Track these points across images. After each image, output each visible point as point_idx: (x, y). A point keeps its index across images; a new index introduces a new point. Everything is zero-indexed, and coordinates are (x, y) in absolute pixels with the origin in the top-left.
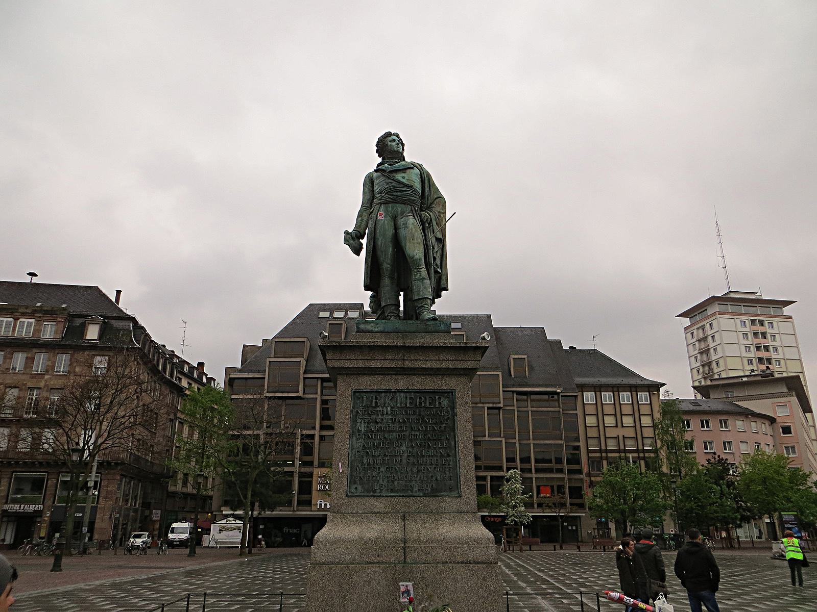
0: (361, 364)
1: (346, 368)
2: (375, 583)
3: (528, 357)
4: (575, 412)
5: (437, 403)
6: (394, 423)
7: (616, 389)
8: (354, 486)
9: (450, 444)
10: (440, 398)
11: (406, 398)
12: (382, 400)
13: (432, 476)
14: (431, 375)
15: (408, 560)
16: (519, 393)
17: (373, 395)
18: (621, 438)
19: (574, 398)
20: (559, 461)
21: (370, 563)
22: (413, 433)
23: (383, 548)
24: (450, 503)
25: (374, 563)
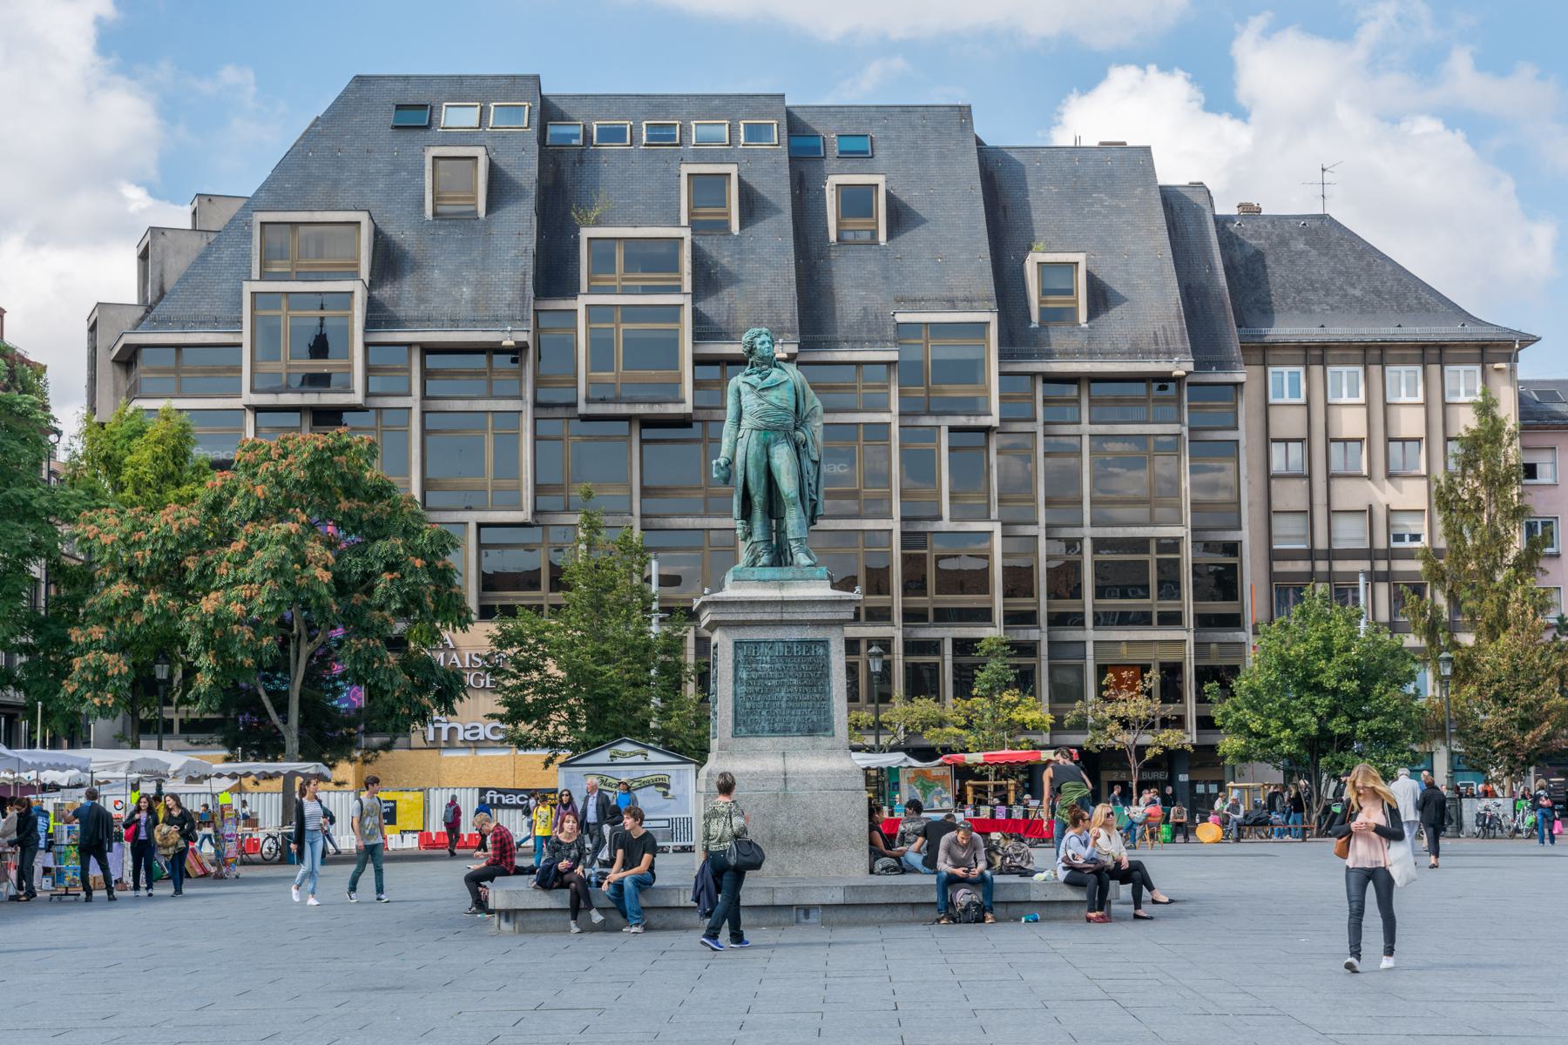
0: (741, 617)
4: (1230, 435)
7: (1374, 354)
15: (789, 788)
16: (1050, 379)
19: (1231, 387)
24: (824, 741)
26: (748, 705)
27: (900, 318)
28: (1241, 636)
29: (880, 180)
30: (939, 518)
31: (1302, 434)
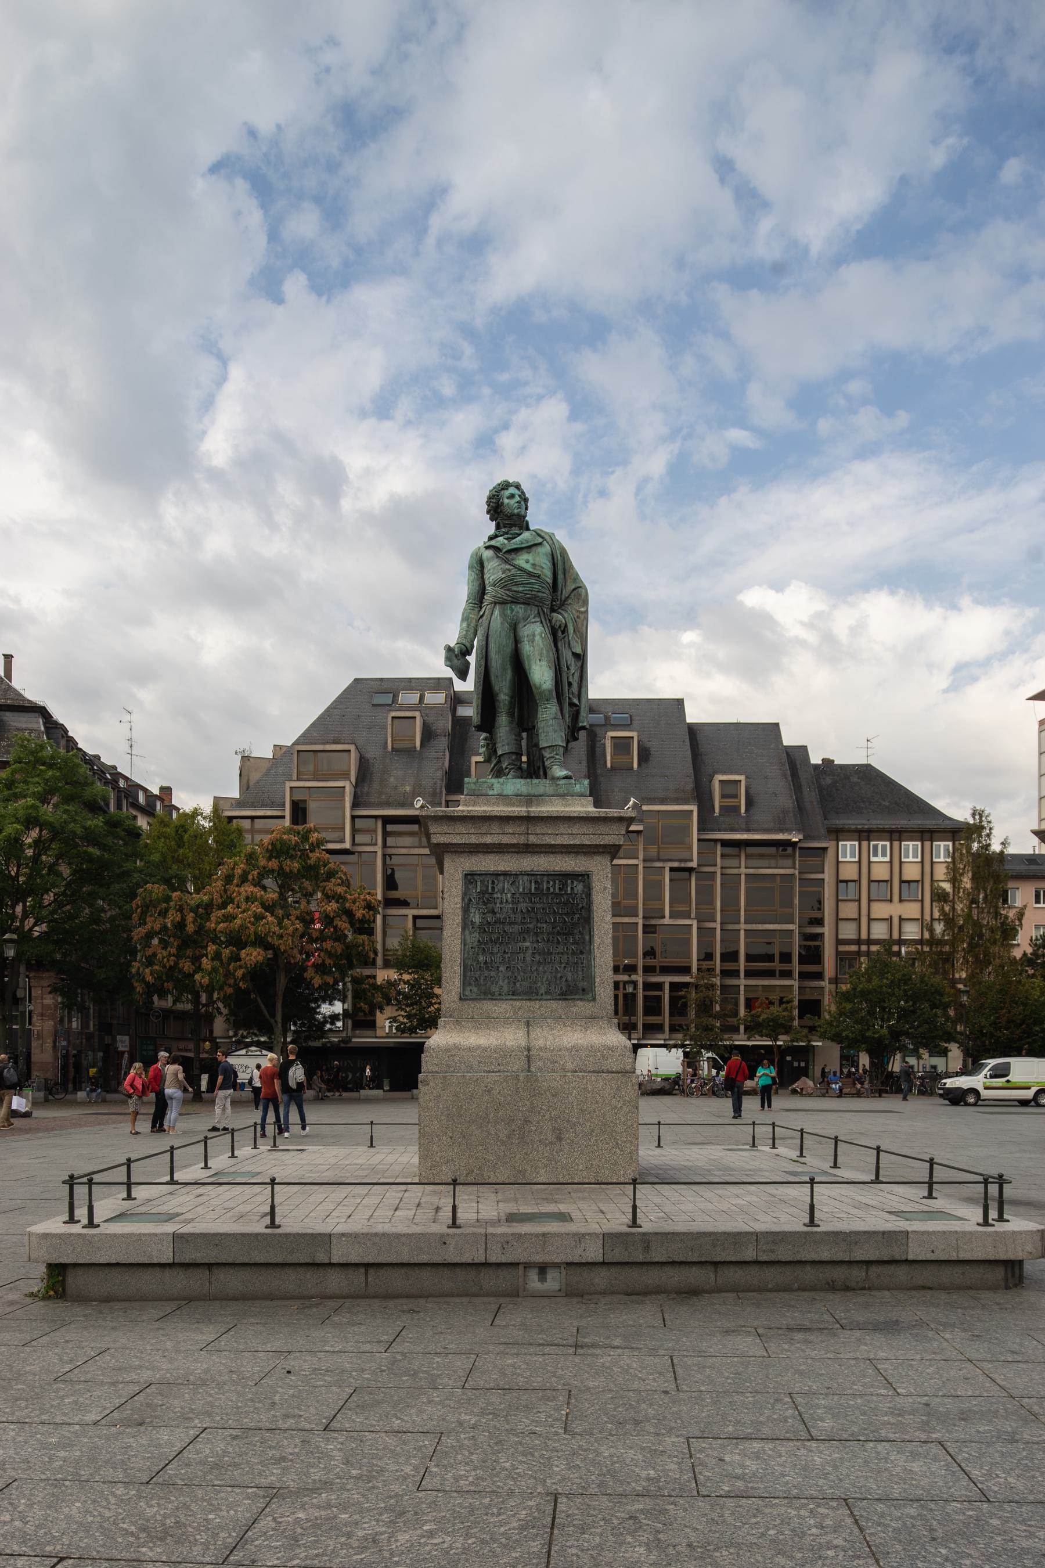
0: (474, 840)
1: (455, 844)
2: (495, 1093)
3: (746, 777)
4: (819, 876)
5: (569, 889)
6: (515, 914)
8: (468, 988)
9: (584, 939)
10: (572, 882)
11: (531, 881)
12: (501, 885)
13: (561, 977)
14: (562, 853)
15: (533, 1069)
16: (725, 843)
17: (488, 878)
18: (896, 921)
20: (786, 957)
21: (489, 1072)
22: (539, 925)
23: (504, 1057)
24: (582, 1007)
25: (493, 1072)
26: (481, 958)
27: (645, 808)
28: (822, 983)
29: (634, 734)
30: (664, 917)
31: (855, 877)
